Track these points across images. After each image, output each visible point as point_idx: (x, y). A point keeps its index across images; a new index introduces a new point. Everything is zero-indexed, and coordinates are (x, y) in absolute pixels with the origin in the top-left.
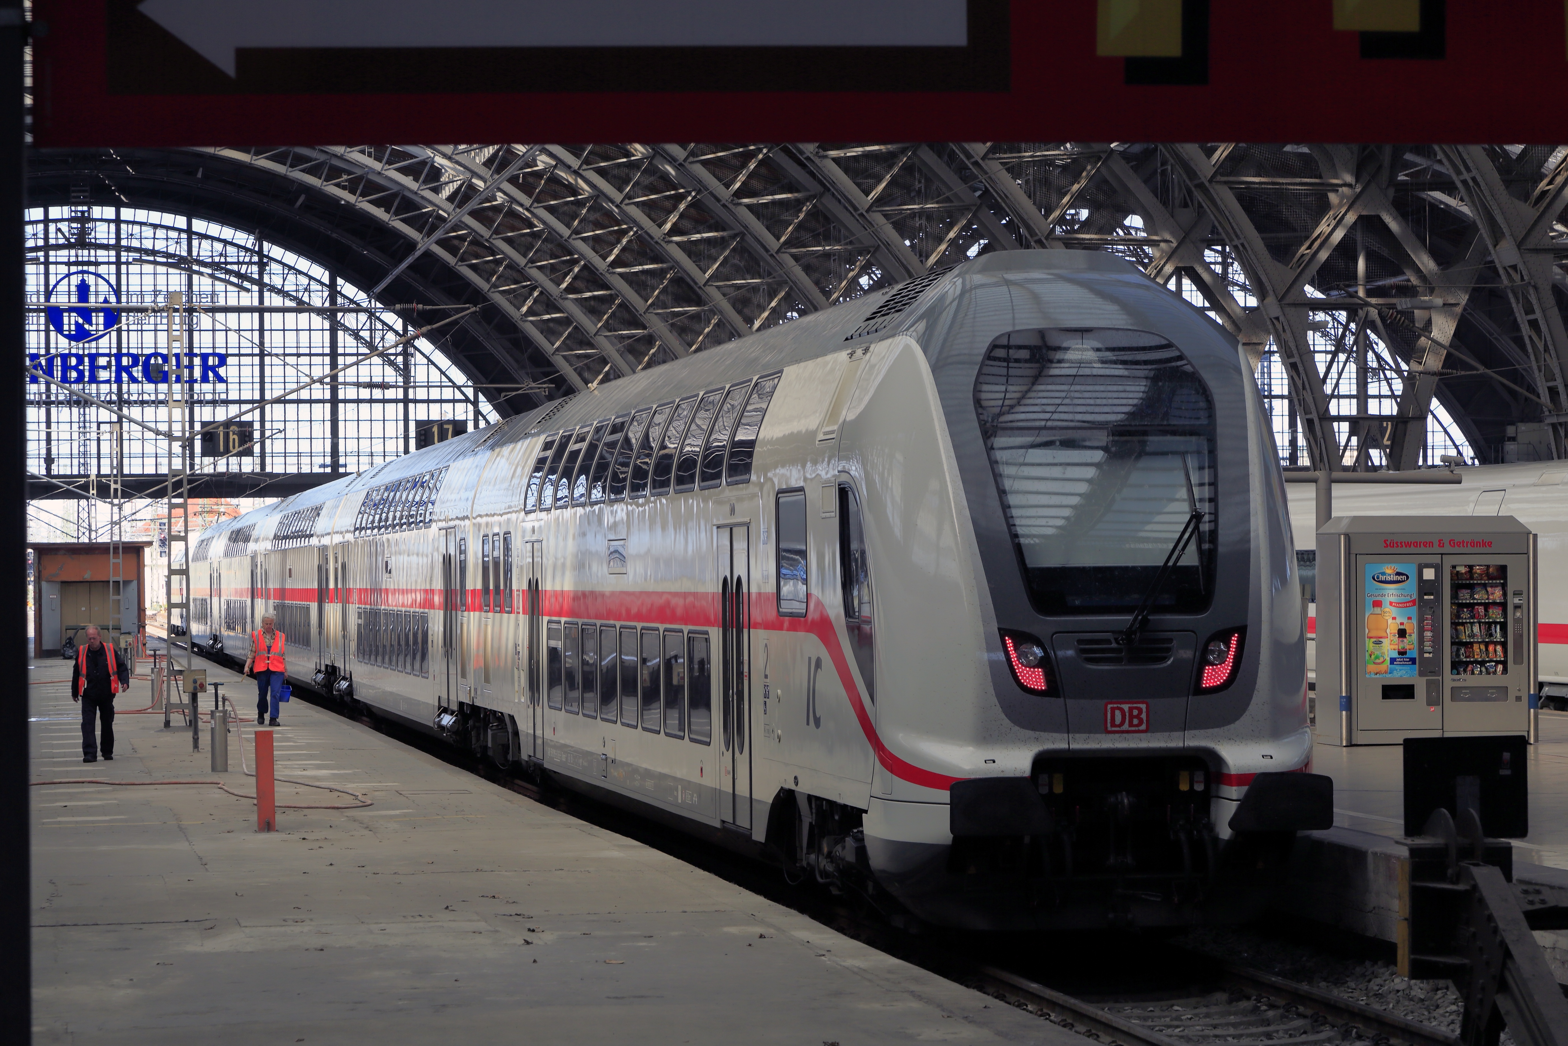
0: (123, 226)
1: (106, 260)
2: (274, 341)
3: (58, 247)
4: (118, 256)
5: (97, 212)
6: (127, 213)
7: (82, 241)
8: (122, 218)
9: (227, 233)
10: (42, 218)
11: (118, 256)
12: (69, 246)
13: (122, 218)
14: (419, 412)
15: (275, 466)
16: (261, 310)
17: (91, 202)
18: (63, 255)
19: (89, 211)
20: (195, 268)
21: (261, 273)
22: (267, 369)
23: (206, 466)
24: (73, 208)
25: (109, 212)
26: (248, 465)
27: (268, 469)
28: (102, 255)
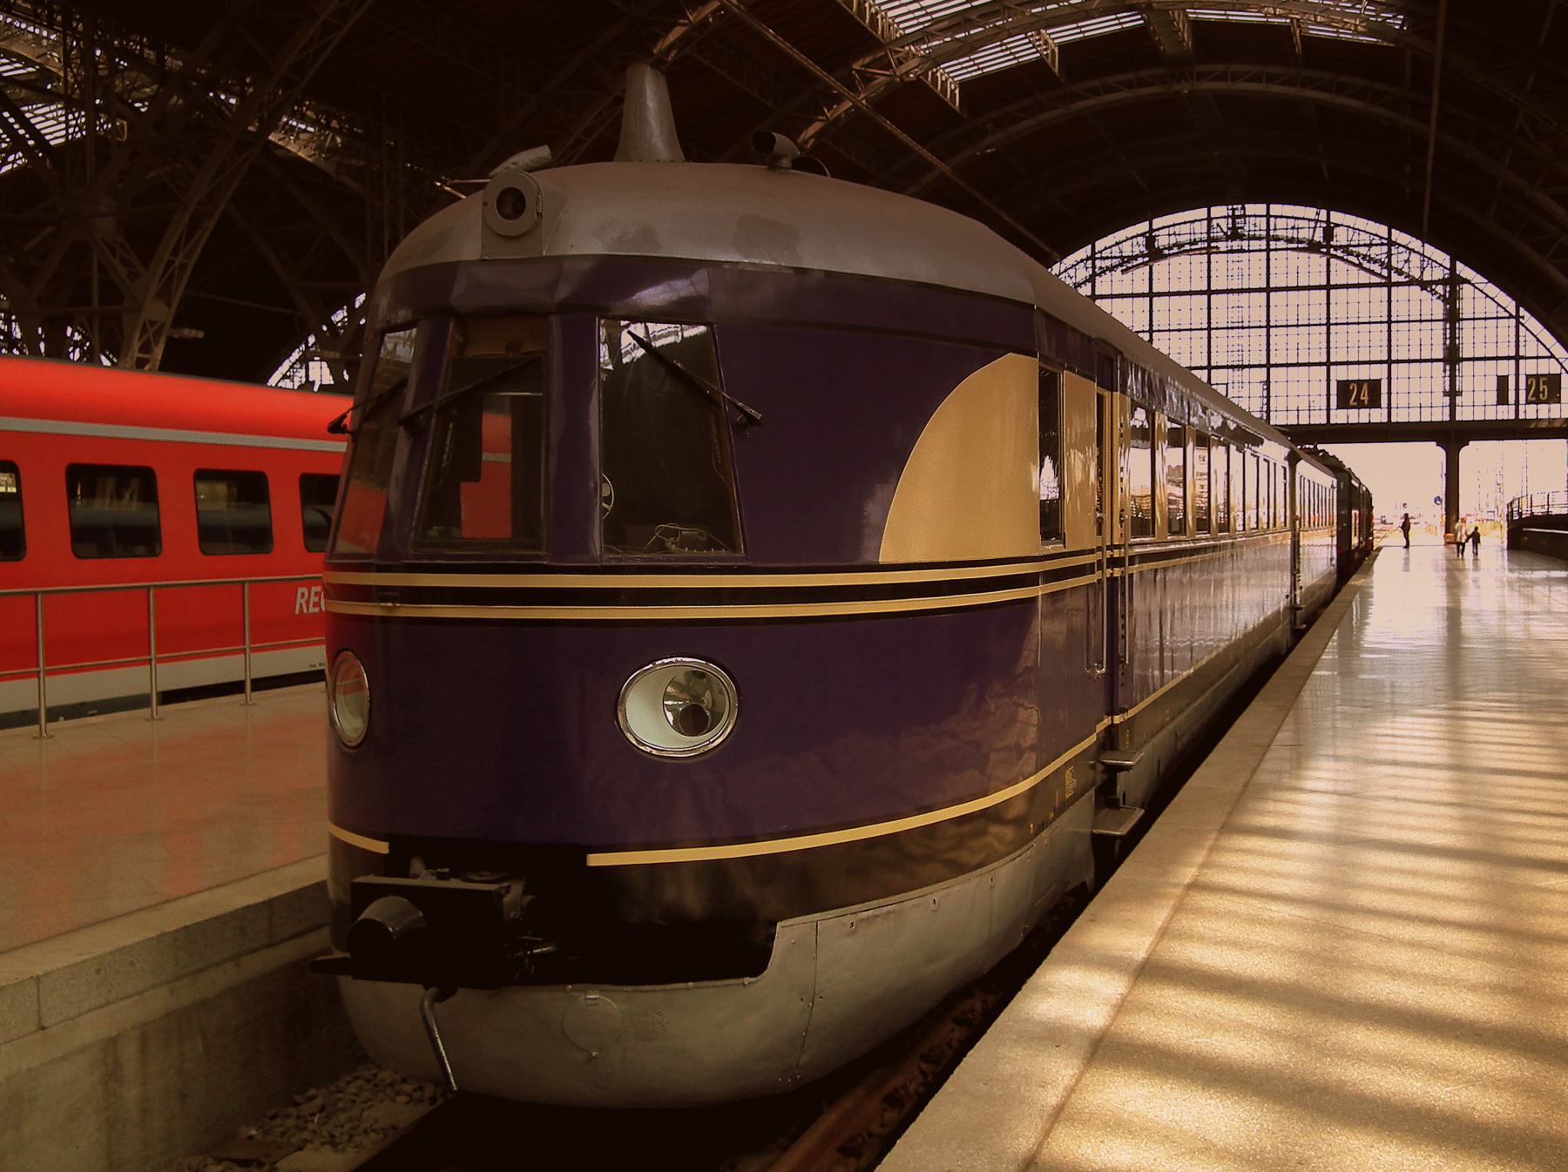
0: (1272, 220)
1: (1258, 248)
2: (1399, 311)
3: (1217, 240)
4: (1268, 245)
5: (1251, 209)
6: (1276, 209)
7: (1234, 234)
8: (1271, 213)
9: (1361, 223)
10: (1206, 217)
11: (1268, 245)
12: (1228, 238)
13: (1271, 213)
14: (1528, 367)
15: (1399, 416)
16: (1389, 284)
17: (1244, 201)
18: (1222, 246)
19: (1243, 208)
20: (1332, 251)
21: (1389, 255)
22: (1393, 334)
23: (1340, 417)
24: (1230, 207)
25: (1260, 209)
26: (1378, 416)
27: (1393, 420)
28: (1255, 245)
